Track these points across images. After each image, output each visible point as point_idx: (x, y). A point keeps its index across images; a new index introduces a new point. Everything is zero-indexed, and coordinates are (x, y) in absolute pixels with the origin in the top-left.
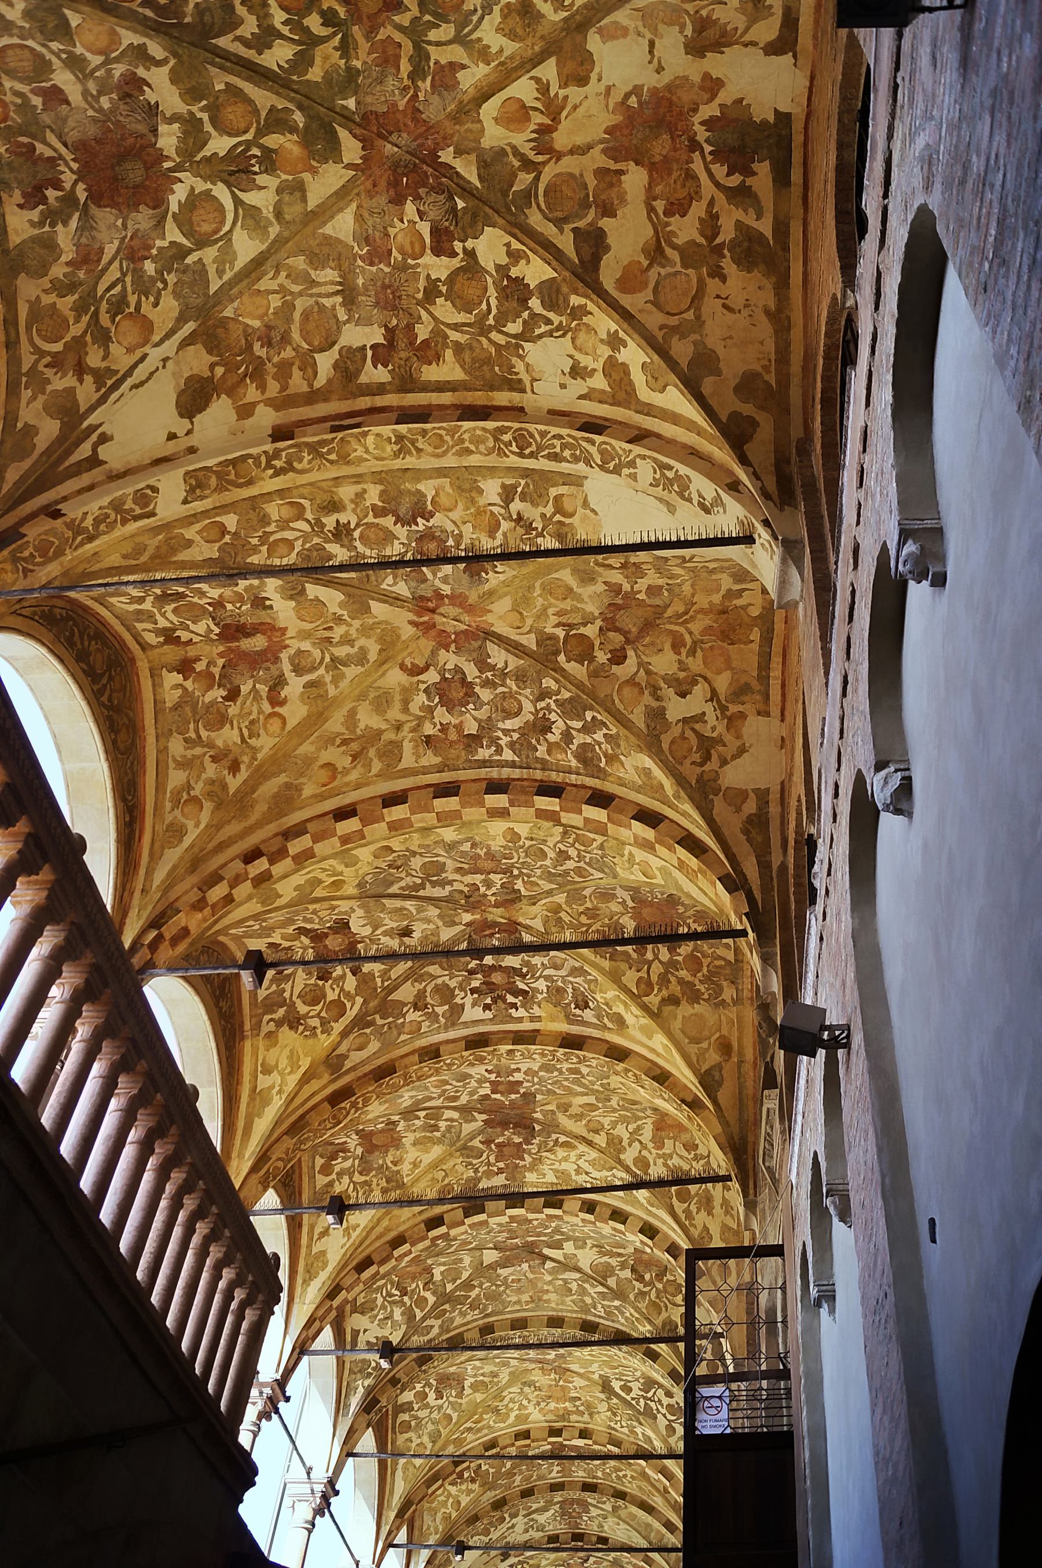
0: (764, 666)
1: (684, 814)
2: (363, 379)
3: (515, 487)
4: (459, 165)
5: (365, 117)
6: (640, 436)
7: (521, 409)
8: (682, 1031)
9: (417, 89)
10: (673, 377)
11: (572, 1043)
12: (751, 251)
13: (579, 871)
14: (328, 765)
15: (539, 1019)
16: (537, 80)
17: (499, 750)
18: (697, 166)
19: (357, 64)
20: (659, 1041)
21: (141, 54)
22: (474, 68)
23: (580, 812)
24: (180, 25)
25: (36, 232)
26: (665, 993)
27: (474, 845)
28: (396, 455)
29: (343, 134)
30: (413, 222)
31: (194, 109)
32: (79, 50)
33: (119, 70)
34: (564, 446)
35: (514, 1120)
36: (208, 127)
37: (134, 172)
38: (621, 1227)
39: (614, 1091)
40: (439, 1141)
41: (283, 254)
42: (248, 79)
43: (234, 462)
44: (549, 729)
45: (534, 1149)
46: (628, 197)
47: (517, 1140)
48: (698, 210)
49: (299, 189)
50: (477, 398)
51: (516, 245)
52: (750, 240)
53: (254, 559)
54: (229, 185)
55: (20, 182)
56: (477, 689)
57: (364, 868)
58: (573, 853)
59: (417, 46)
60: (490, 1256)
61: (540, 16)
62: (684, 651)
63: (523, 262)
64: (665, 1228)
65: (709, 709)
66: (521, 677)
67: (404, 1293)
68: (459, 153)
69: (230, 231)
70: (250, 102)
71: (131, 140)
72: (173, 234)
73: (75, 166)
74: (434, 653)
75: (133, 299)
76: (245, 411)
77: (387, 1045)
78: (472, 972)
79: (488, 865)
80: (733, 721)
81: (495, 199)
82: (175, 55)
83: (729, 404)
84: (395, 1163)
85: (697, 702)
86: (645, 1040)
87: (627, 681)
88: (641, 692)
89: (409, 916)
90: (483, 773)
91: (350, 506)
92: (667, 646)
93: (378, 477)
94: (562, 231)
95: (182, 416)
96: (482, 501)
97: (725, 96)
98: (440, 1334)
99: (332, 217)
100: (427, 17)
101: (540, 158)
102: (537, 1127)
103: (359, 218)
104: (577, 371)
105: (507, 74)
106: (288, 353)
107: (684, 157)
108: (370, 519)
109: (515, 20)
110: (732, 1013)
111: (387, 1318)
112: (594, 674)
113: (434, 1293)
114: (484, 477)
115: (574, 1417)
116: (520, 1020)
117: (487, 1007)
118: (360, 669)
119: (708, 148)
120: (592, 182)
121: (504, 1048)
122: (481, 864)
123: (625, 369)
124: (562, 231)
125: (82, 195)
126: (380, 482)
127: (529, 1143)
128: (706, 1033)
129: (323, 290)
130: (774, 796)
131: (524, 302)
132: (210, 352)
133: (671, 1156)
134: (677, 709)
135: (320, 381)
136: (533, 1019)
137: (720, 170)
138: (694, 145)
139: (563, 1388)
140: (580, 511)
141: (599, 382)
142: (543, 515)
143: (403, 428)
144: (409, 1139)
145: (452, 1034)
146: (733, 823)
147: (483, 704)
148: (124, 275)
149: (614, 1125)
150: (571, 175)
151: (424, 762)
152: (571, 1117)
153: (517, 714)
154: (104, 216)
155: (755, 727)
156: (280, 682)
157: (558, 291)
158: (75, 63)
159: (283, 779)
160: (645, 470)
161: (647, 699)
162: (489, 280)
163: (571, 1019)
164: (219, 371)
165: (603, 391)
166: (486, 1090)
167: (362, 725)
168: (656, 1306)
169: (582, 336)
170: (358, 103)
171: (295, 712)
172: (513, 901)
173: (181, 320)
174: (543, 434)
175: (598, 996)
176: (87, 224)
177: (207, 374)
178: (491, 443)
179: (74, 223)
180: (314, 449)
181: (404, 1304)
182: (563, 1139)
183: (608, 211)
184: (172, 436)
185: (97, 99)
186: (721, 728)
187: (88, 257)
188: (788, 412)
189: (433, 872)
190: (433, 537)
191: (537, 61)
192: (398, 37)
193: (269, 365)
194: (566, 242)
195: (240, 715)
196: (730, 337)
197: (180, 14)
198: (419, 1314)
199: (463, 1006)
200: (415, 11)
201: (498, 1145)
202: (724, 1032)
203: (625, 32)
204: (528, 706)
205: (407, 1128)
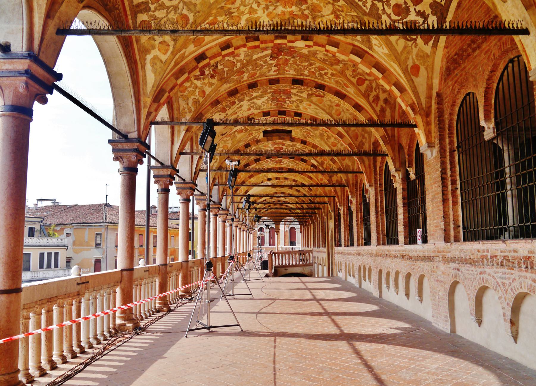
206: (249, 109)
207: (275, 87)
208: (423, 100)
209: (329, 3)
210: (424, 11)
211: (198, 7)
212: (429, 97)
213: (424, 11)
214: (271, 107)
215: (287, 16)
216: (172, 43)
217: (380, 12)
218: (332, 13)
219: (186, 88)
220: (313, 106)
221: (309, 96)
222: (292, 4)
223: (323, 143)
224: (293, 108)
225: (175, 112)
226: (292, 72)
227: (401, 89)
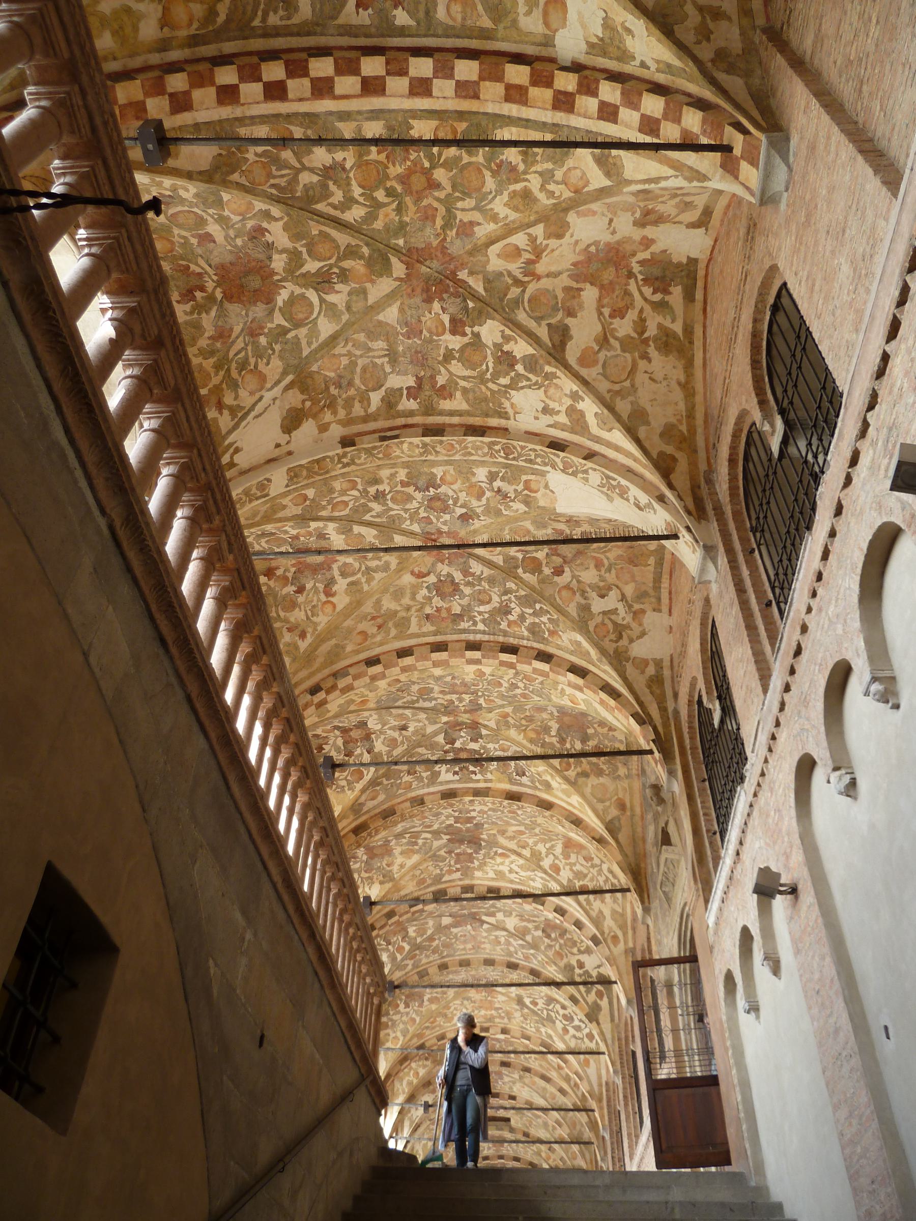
0: (657, 580)
1: (604, 671)
2: (400, 407)
3: (497, 473)
4: (471, 281)
5: (409, 250)
6: (590, 456)
7: (506, 429)
8: (592, 794)
9: (446, 235)
10: (617, 425)
11: (513, 797)
12: (668, 343)
13: (524, 696)
14: (363, 633)
15: (490, 781)
16: (529, 235)
17: (475, 624)
18: (632, 287)
19: (407, 219)
20: (575, 799)
21: (267, 215)
22: (486, 226)
23: (530, 664)
24: (293, 197)
25: (188, 318)
26: (579, 769)
27: (453, 678)
28: (421, 454)
29: (394, 260)
30: (439, 313)
31: (297, 245)
32: (226, 213)
33: (250, 224)
34: (537, 456)
35: (468, 840)
36: (305, 256)
37: (255, 282)
38: (541, 907)
39: (539, 825)
40: (418, 852)
41: (351, 332)
42: (334, 228)
43: (318, 461)
44: (510, 613)
45: (481, 857)
46: (585, 305)
47: (469, 851)
48: (632, 315)
49: (364, 292)
50: (477, 421)
51: (508, 332)
52: (667, 336)
53: (324, 513)
54: (316, 290)
55: (177, 287)
56: (462, 587)
57: (381, 692)
58: (521, 685)
59: (448, 211)
60: (446, 921)
61: (536, 200)
62: (603, 570)
63: (512, 342)
64: (571, 909)
65: (620, 606)
66: (491, 581)
67: (389, 943)
68: (471, 273)
69: (317, 318)
70: (334, 241)
71: (254, 264)
72: (279, 320)
73: (215, 278)
74: (433, 565)
75: (252, 361)
76: (323, 428)
77: (389, 797)
78: (446, 752)
79: (462, 689)
80: (637, 615)
81: (496, 302)
82: (288, 215)
83: (658, 446)
84: (388, 865)
85: (612, 601)
86: (564, 797)
87: (564, 587)
88: (574, 593)
89: (407, 719)
90: (463, 637)
91: (386, 481)
92: (592, 566)
93: (406, 465)
94: (540, 325)
95: (284, 432)
96: (474, 480)
97: (654, 248)
99: (383, 310)
100: (457, 194)
101: (526, 279)
102: (483, 844)
103: (401, 310)
104: (546, 410)
105: (510, 230)
106: (352, 392)
107: (624, 281)
108: (399, 488)
109: (518, 201)
110: (625, 784)
112: (542, 581)
113: (409, 944)
114: (477, 467)
115: (497, 1020)
116: (478, 781)
117: (455, 773)
118: (385, 574)
119: (640, 277)
120: (560, 295)
121: (467, 799)
122: (457, 689)
123: (582, 414)
124: (540, 325)
125: (219, 295)
126: (408, 467)
127: (477, 853)
128: (608, 796)
129: (376, 353)
130: (666, 664)
131: (512, 366)
132: (302, 393)
133: (575, 864)
134: (598, 605)
135: (373, 408)
136: (486, 781)
137: (648, 291)
138: (631, 275)
139: (490, 1002)
140: (542, 490)
141: (563, 419)
142: (516, 490)
143: (427, 439)
144: (397, 851)
145: (432, 789)
146: (640, 682)
147: (465, 596)
148: (247, 345)
149: (536, 844)
150: (547, 290)
151: (425, 629)
152: (506, 838)
153: (488, 603)
154: (234, 309)
155: (651, 619)
156: (331, 582)
157: (536, 362)
158: (222, 220)
159: (333, 642)
160: (595, 478)
161: (578, 598)
162: (489, 352)
163: (511, 781)
164: (308, 404)
165: (565, 425)
166: (451, 821)
167: (384, 608)
168: (559, 955)
169: (552, 391)
170: (405, 242)
171: (341, 600)
172: (476, 710)
173: (285, 373)
174: (522, 448)
175: (532, 769)
176: (222, 313)
177: (300, 406)
178: (486, 450)
179: (213, 313)
180: (369, 451)
181: (388, 950)
182: (500, 851)
183: (571, 313)
184: (278, 446)
185: (234, 239)
186: (629, 619)
187: (222, 334)
188: (695, 451)
189: (425, 693)
190: (439, 499)
191: (530, 225)
192: (436, 204)
193: (339, 400)
194: (543, 332)
195: (305, 602)
196: (655, 400)
197: (293, 191)
198: (399, 957)
199: (439, 772)
200: (449, 189)
201: (457, 854)
202: (621, 796)
203: (594, 213)
204: (495, 598)
205: (397, 844)
208: (596, 1088)
212: (600, 1085)
216: (401, 1038)
220: (526, 1088)
221: (521, 1077)
227: (580, 1078)
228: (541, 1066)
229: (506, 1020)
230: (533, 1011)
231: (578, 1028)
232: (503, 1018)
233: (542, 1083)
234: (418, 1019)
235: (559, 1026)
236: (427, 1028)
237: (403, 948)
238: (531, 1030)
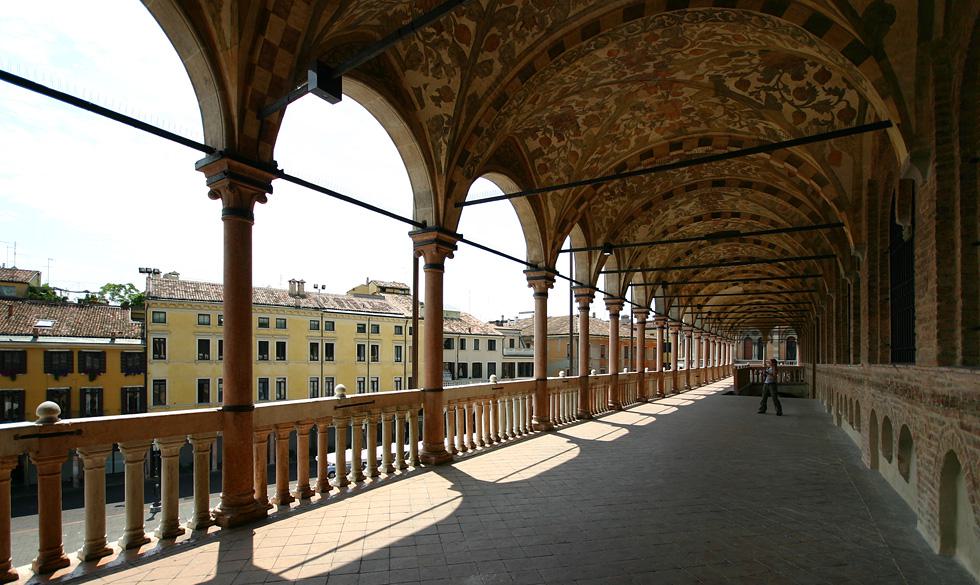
98: (506, 70)
111: (437, 66)
113: (471, 17)
115: (691, 129)
139: (674, 103)
198: (467, 50)
206: (677, 217)
207: (693, 193)
209: (717, 105)
210: (836, 88)
211: (585, 142)
213: (836, 88)
214: (702, 211)
215: (677, 127)
217: (780, 101)
218: (725, 114)
219: (599, 210)
222: (679, 116)
223: (780, 241)
224: (728, 208)
225: (592, 234)
226: (709, 174)
228: (764, 177)
229: (703, 127)
230: (741, 98)
231: (825, 107)
232: (698, 124)
233: (768, 196)
234: (579, 152)
235: (788, 110)
236: (597, 160)
237: (466, 28)
238: (742, 130)
